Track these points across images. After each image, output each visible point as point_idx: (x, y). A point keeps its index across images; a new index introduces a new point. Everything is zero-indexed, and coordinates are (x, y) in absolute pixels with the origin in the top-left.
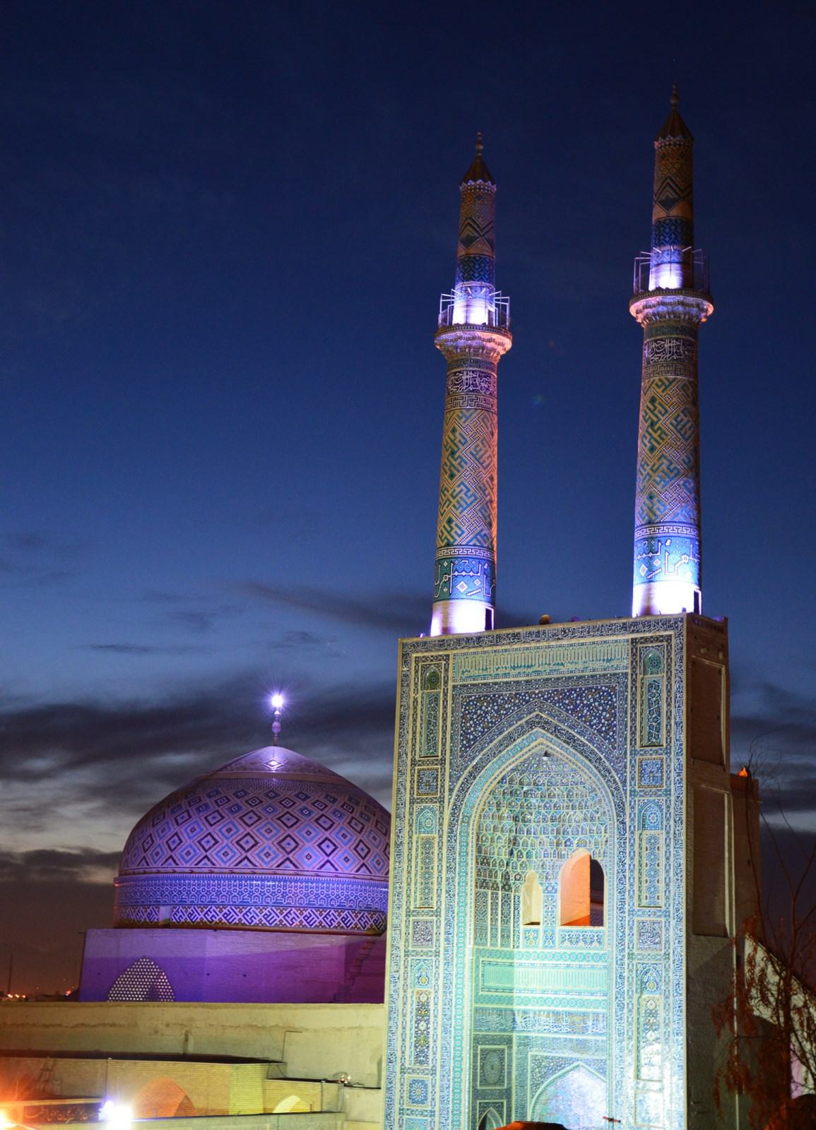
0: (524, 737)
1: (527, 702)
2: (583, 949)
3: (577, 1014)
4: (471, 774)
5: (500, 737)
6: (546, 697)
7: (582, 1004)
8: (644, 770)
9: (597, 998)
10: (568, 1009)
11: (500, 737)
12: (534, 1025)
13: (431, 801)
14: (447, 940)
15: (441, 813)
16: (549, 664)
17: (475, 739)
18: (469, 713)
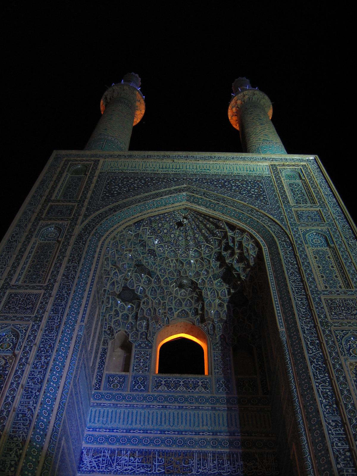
1: (175, 181)
2: (184, 392)
3: (176, 453)
4: (110, 209)
5: (146, 194)
6: (194, 180)
7: (183, 443)
8: (301, 215)
9: (203, 437)
10: (163, 448)
11: (146, 194)
12: (111, 466)
13: (62, 219)
14: (55, 310)
15: (72, 227)
16: (196, 169)
17: (119, 194)
18: (114, 183)
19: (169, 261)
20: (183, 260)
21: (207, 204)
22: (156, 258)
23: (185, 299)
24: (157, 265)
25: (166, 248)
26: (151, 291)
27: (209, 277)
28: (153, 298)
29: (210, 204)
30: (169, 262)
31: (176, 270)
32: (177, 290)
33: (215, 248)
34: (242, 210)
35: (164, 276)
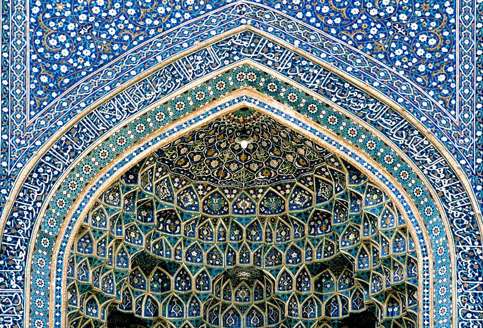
0: (212, 75)
19: (208, 222)
20: (240, 220)
21: (299, 102)
22: (177, 222)
23: (247, 307)
24: (180, 243)
25: (201, 193)
26: (170, 304)
27: (301, 268)
28: (175, 323)
29: (307, 104)
30: (209, 225)
31: (225, 246)
32: (228, 285)
33: (320, 199)
34: (384, 132)
35: (197, 268)
